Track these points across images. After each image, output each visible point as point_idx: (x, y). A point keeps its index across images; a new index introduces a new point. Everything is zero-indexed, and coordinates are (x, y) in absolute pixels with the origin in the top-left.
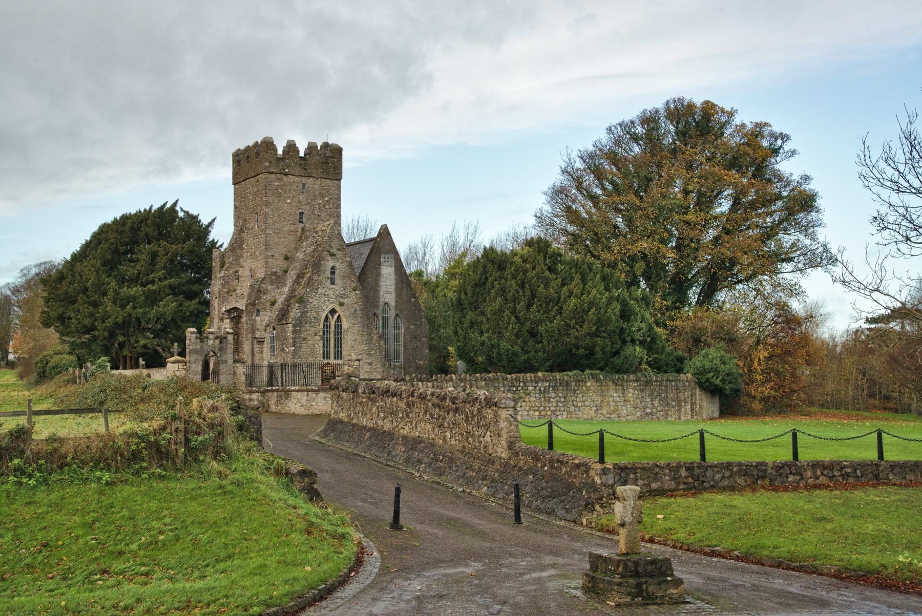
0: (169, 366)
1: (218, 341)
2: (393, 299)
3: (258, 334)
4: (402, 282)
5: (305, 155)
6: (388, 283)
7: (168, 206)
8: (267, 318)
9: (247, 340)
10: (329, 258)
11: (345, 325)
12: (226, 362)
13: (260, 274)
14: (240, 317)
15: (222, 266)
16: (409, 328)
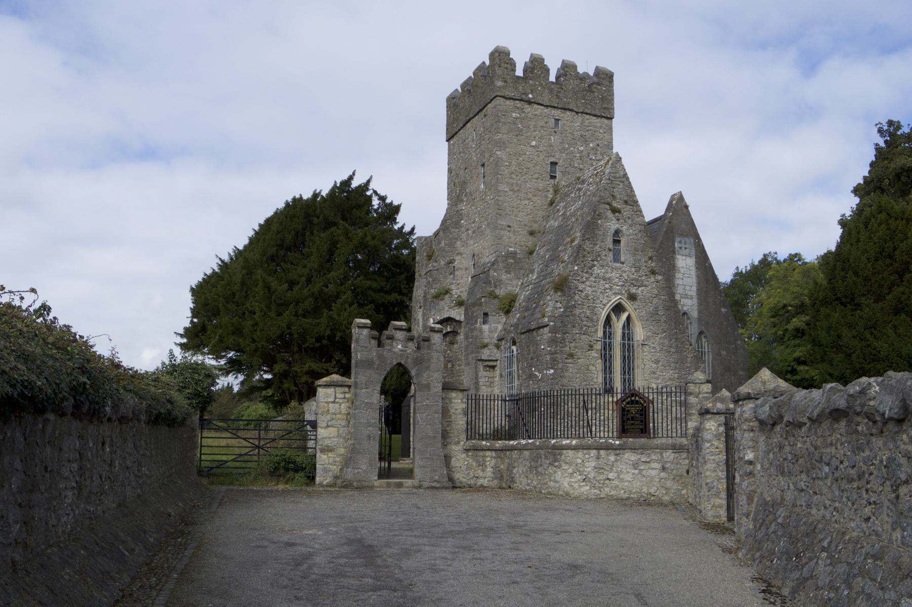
0: (321, 392)
1: (412, 346)
2: (695, 308)
3: (485, 354)
4: (707, 281)
5: (557, 78)
6: (687, 281)
7: (355, 184)
8: (500, 327)
9: (468, 364)
10: (609, 214)
11: (639, 333)
12: (428, 387)
13: (488, 258)
14: (455, 333)
15: (430, 257)
16: (719, 354)
